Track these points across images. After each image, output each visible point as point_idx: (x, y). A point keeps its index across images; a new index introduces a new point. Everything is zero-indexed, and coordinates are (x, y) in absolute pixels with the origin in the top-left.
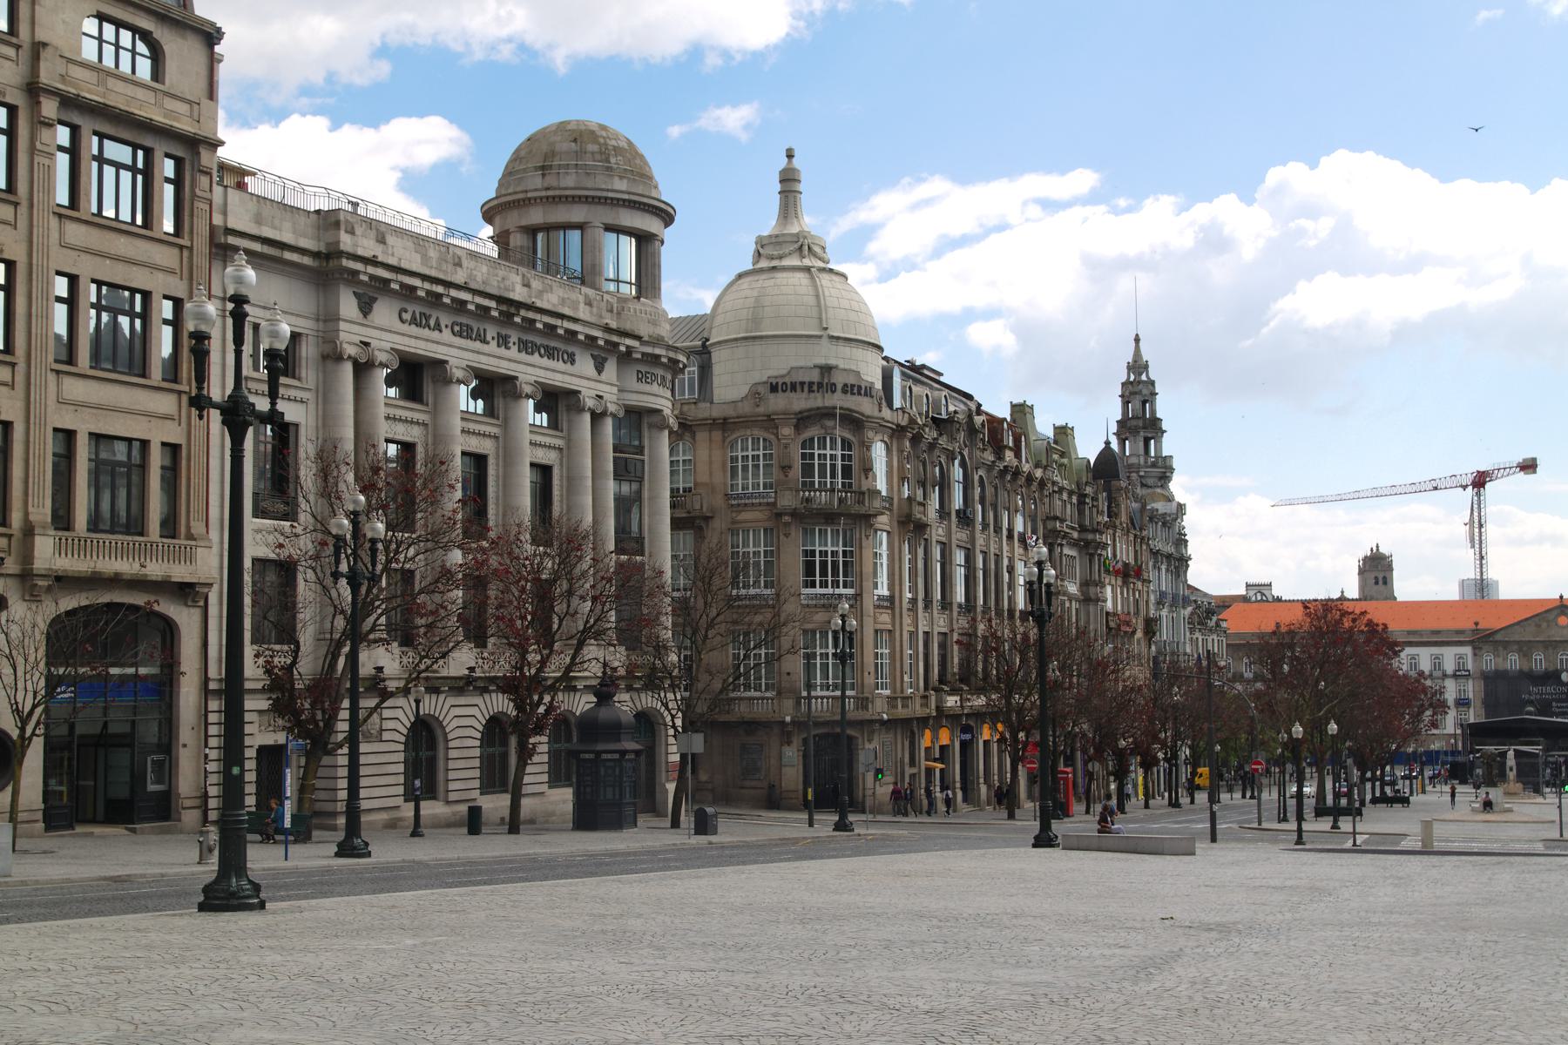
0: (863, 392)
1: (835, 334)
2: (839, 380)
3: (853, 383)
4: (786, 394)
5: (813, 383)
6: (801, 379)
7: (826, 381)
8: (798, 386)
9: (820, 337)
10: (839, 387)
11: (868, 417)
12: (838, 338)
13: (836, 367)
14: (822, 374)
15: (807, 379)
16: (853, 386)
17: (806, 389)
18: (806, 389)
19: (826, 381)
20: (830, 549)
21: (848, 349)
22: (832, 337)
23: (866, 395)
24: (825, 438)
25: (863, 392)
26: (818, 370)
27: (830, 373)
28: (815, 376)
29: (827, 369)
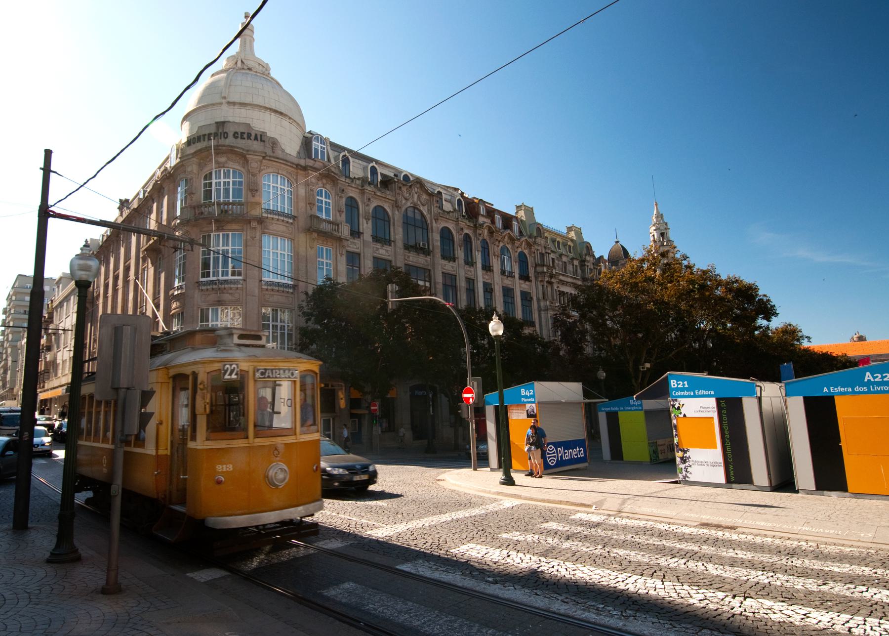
0: (253, 137)
1: (231, 100)
2: (231, 130)
3: (243, 131)
4: (195, 145)
5: (211, 134)
6: (204, 133)
7: (220, 131)
8: (202, 138)
9: (221, 104)
10: (231, 135)
11: (248, 151)
12: (234, 104)
13: (229, 122)
14: (218, 128)
15: (207, 132)
16: (242, 133)
17: (206, 138)
18: (206, 138)
19: (220, 131)
20: (221, 248)
21: (243, 110)
22: (229, 103)
23: (256, 138)
24: (220, 171)
25: (253, 137)
26: (215, 125)
27: (223, 126)
28: (213, 130)
29: (221, 124)
